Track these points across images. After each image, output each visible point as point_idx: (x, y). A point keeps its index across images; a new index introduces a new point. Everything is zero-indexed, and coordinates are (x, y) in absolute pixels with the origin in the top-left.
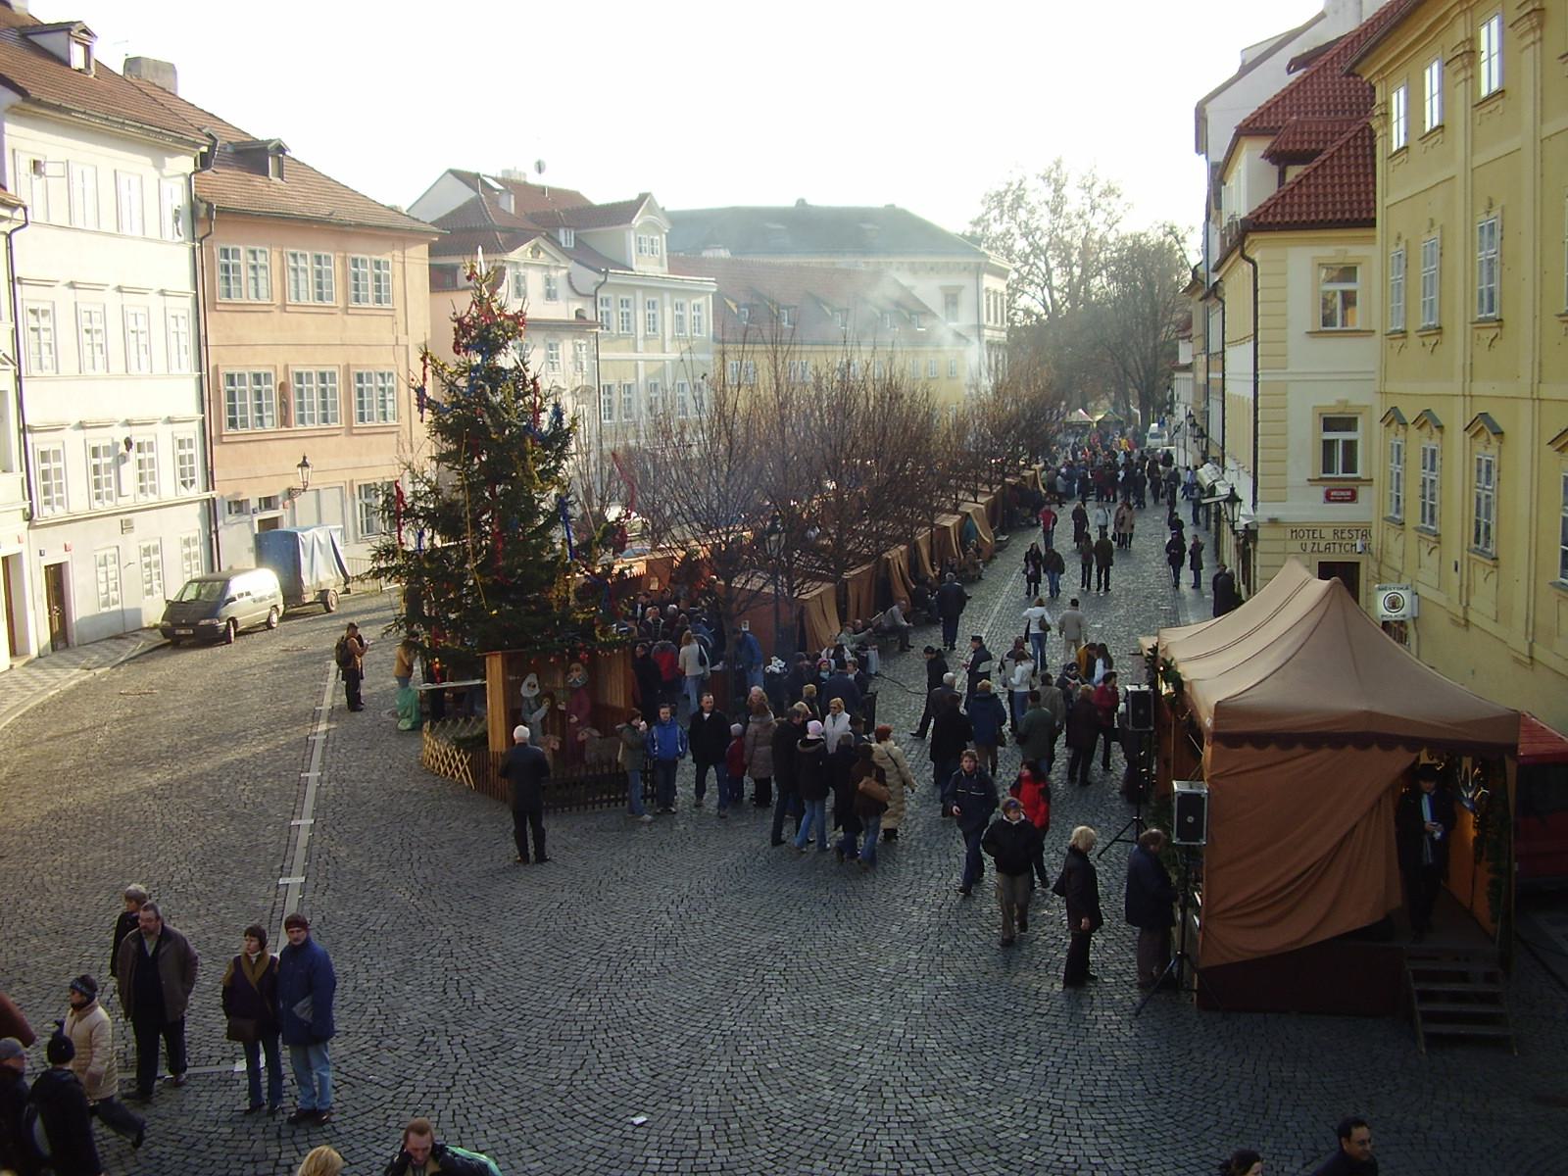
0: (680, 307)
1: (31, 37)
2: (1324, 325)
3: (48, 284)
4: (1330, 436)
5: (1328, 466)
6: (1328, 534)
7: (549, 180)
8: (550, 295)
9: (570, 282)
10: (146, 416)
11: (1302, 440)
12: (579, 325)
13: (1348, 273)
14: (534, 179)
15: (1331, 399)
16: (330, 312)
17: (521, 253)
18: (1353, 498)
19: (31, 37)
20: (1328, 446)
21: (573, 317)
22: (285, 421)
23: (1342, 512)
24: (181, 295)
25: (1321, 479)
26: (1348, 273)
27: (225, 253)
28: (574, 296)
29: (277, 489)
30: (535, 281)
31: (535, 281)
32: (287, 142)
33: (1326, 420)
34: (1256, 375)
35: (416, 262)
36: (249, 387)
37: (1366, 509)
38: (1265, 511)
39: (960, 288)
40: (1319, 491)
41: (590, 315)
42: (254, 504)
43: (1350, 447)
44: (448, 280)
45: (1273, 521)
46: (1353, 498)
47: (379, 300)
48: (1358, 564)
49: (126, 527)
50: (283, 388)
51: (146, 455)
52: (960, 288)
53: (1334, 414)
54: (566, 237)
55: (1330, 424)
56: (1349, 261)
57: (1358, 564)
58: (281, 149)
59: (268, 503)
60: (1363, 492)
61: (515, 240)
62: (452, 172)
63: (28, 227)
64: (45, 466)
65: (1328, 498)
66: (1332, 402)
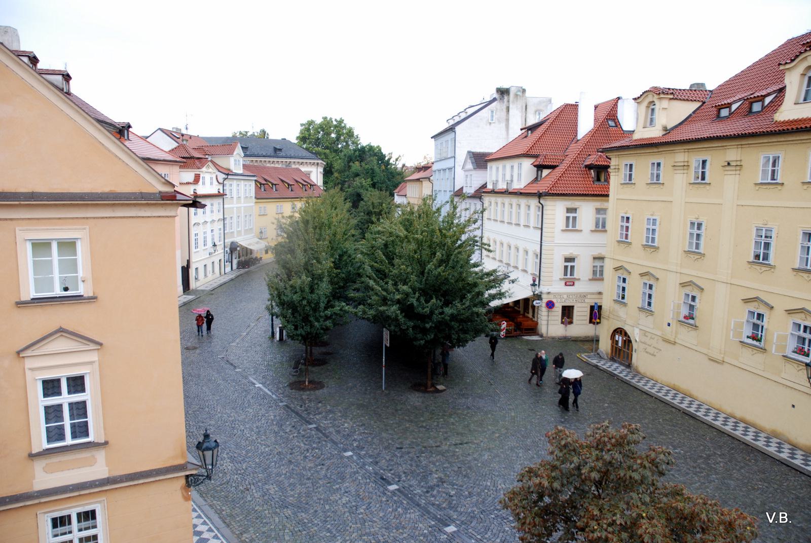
0: (246, 185)
5: (566, 274)
6: (565, 296)
8: (211, 184)
9: (217, 179)
11: (560, 264)
12: (220, 195)
13: (574, 210)
14: (184, 132)
15: (568, 252)
17: (204, 169)
18: (573, 285)
20: (566, 267)
21: (217, 193)
23: (570, 289)
25: (564, 279)
26: (574, 210)
32: (132, 124)
33: (565, 259)
34: (541, 242)
37: (579, 288)
40: (563, 282)
41: (221, 192)
43: (572, 267)
45: (549, 293)
46: (573, 285)
48: (573, 307)
53: (568, 256)
55: (568, 260)
56: (576, 207)
57: (573, 307)
60: (576, 283)
62: (160, 129)
65: (566, 284)
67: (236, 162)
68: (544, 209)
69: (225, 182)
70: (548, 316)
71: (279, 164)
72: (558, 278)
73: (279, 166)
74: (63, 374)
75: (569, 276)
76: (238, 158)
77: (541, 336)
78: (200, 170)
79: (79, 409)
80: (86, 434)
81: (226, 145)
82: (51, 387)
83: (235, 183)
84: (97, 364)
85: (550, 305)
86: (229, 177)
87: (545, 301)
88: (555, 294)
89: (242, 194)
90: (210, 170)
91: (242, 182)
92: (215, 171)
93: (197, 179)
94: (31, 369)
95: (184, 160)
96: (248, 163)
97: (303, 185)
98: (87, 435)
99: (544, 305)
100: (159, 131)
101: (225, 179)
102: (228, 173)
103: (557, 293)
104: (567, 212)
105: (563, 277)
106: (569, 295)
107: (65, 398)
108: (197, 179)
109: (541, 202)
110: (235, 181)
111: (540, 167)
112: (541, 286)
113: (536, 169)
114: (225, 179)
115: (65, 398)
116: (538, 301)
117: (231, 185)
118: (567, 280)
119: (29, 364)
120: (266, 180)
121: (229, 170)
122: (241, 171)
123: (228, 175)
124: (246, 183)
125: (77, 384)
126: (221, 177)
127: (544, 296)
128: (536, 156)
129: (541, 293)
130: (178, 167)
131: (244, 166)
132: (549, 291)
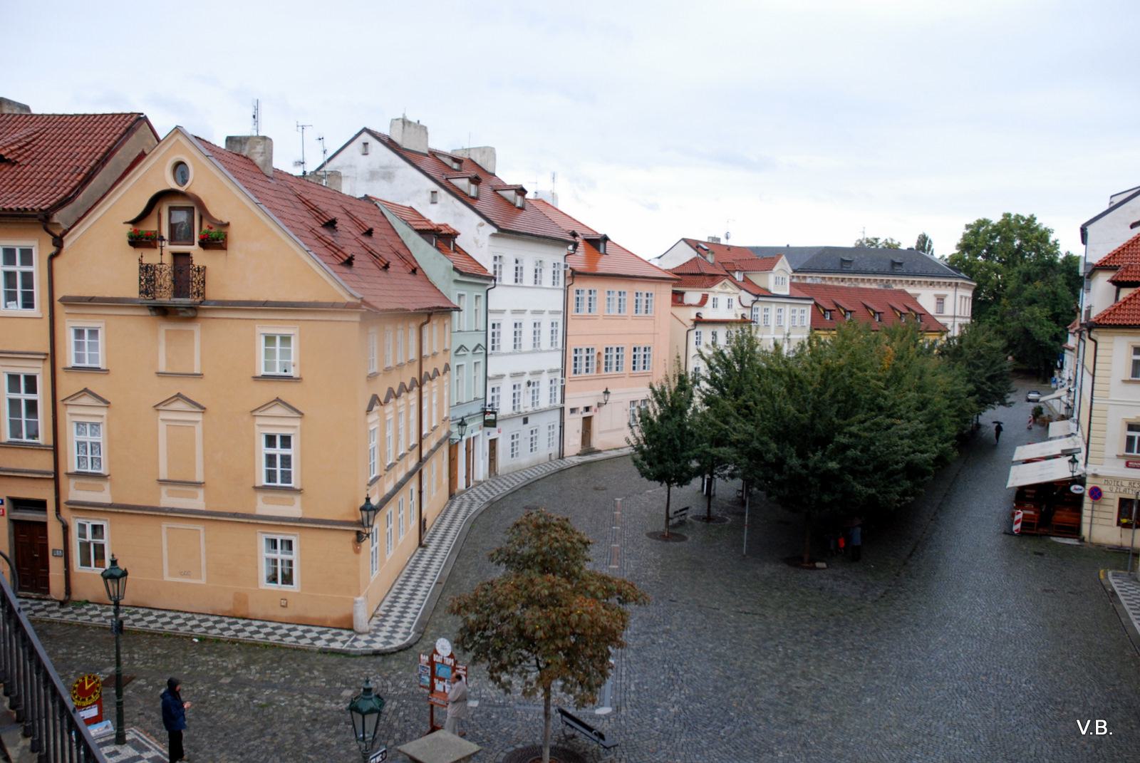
1: (499, 192)
2: (1132, 376)
3: (502, 312)
4: (1132, 434)
6: (1126, 484)
7: (731, 242)
9: (740, 301)
10: (536, 368)
14: (723, 242)
16: (624, 318)
17: (717, 288)
19: (499, 192)
22: (598, 369)
24: (558, 312)
25: (1124, 456)
27: (578, 292)
28: (741, 307)
29: (592, 402)
30: (723, 300)
31: (723, 300)
32: (610, 236)
35: (666, 292)
36: (584, 354)
38: (1090, 470)
39: (946, 296)
40: (1123, 462)
42: (582, 409)
44: (679, 299)
45: (1095, 476)
47: (647, 312)
49: (526, 421)
50: (599, 353)
51: (536, 388)
52: (946, 296)
54: (738, 276)
58: (605, 239)
59: (587, 409)
61: (714, 279)
62: (684, 239)
63: (497, 288)
64: (493, 394)
65: (1127, 465)
66: (1134, 418)
67: (778, 280)
68: (1099, 347)
69: (755, 306)
70: (1093, 510)
71: (871, 284)
72: (1114, 455)
73: (846, 285)
74: (278, 432)
75: (1135, 453)
76: (782, 274)
77: (1082, 540)
78: (708, 289)
79: (286, 460)
80: (290, 482)
81: (765, 258)
82: (271, 440)
83: (773, 309)
84: (299, 428)
85: (1096, 494)
86: (760, 299)
87: (1088, 486)
88: (1108, 480)
89: (787, 322)
90: (729, 290)
91: (788, 306)
92: (737, 290)
93: (704, 300)
94: (259, 425)
95: (679, 277)
96: (795, 280)
97: (901, 313)
98: (290, 483)
99: (1087, 493)
100: (682, 242)
101: (754, 302)
102: (762, 294)
103: (1111, 477)
104: (1135, 354)
105: (1122, 451)
106: (1132, 482)
107: (278, 451)
108: (704, 300)
109: (1093, 335)
110: (774, 305)
111: (1119, 284)
112: (1088, 465)
113: (1115, 288)
114: (754, 302)
115: (278, 451)
116: (1078, 487)
117: (766, 310)
118: (1129, 459)
119: (259, 421)
120: (837, 305)
121: (767, 290)
122: (787, 293)
123: (757, 296)
124: (794, 307)
125: (286, 441)
126: (747, 298)
127: (1089, 480)
128: (1114, 269)
129: (1085, 474)
130: (671, 286)
131: (792, 284)
132: (1096, 472)
